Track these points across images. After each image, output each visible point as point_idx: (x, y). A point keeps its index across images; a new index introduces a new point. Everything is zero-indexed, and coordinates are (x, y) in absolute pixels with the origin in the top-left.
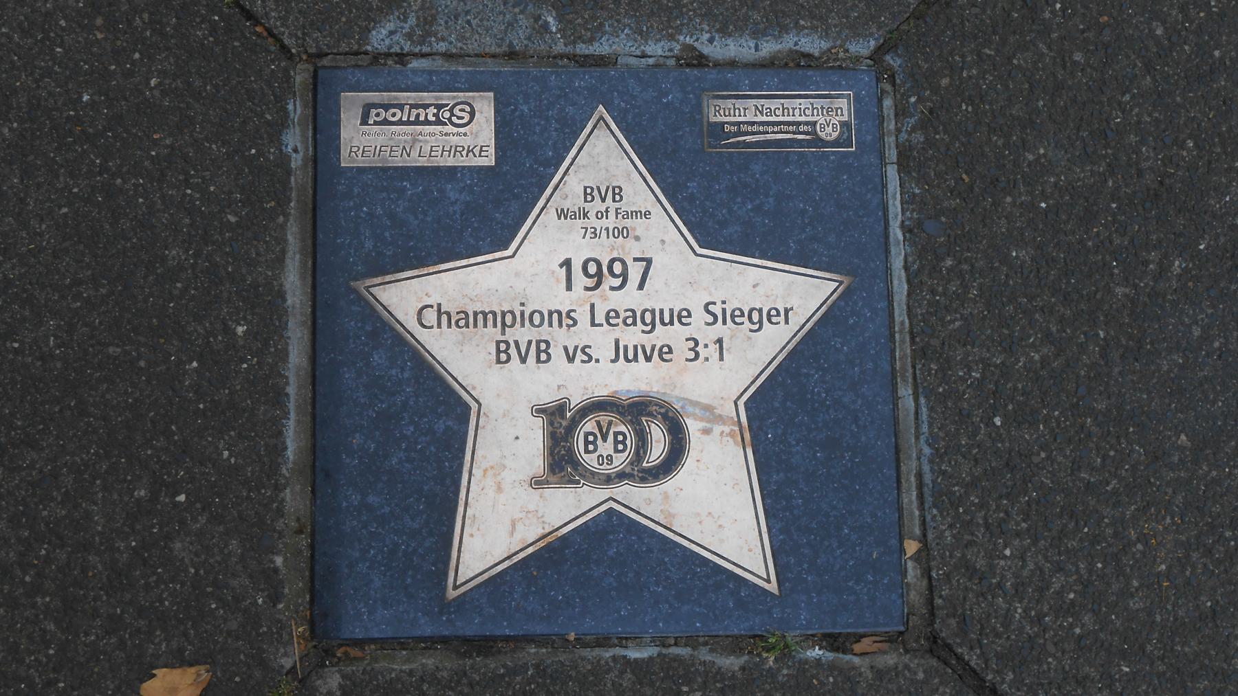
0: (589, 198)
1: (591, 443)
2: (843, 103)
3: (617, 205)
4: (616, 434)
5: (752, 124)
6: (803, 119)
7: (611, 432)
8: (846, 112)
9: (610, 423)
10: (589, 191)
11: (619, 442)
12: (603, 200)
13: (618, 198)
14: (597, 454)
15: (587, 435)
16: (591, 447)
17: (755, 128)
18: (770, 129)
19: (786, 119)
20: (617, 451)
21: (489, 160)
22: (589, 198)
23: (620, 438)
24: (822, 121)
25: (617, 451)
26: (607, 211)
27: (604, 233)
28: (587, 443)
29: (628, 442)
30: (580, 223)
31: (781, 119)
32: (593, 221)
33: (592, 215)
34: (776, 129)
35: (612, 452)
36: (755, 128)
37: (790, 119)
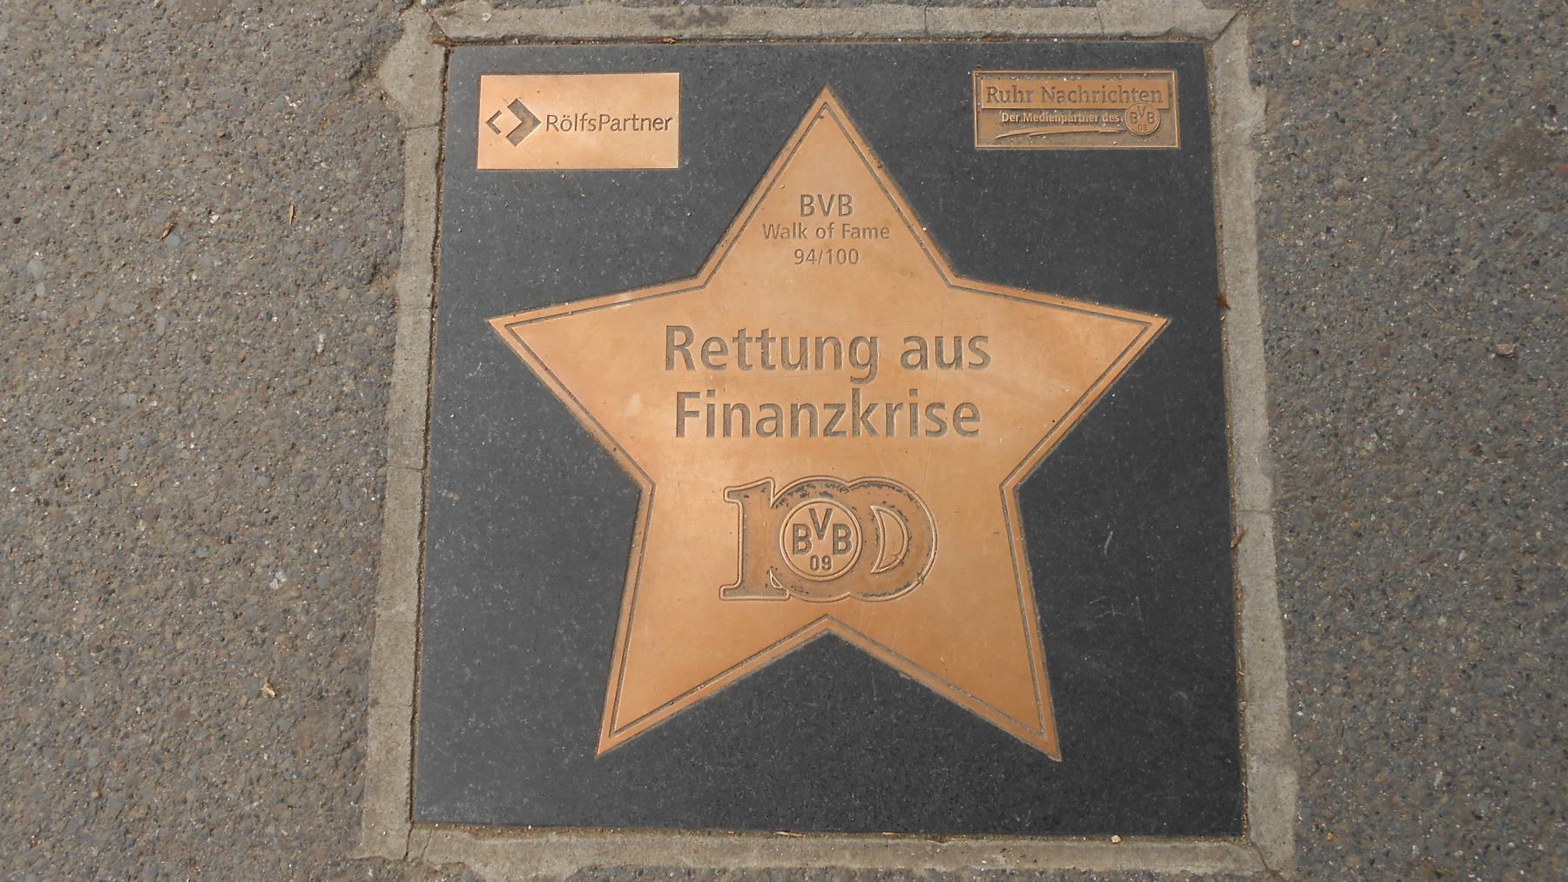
0: (807, 210)
1: (801, 539)
2: (1162, 82)
3: (845, 219)
4: (835, 526)
5: (1040, 111)
6: (1109, 105)
7: (828, 531)
8: (1165, 97)
9: (827, 514)
10: (807, 200)
11: (840, 541)
12: (827, 214)
13: (844, 210)
14: (810, 553)
15: (796, 527)
16: (801, 545)
17: (1044, 117)
18: (1061, 118)
19: (1083, 105)
20: (836, 551)
21: (674, 164)
22: (807, 210)
23: (841, 533)
24: (1134, 109)
25: (836, 551)
26: (830, 228)
27: (825, 256)
28: (796, 539)
29: (852, 539)
30: (796, 243)
31: (1076, 106)
32: (810, 242)
33: (810, 233)
34: (1070, 118)
35: (830, 553)
36: (1044, 117)
37: (1091, 105)
